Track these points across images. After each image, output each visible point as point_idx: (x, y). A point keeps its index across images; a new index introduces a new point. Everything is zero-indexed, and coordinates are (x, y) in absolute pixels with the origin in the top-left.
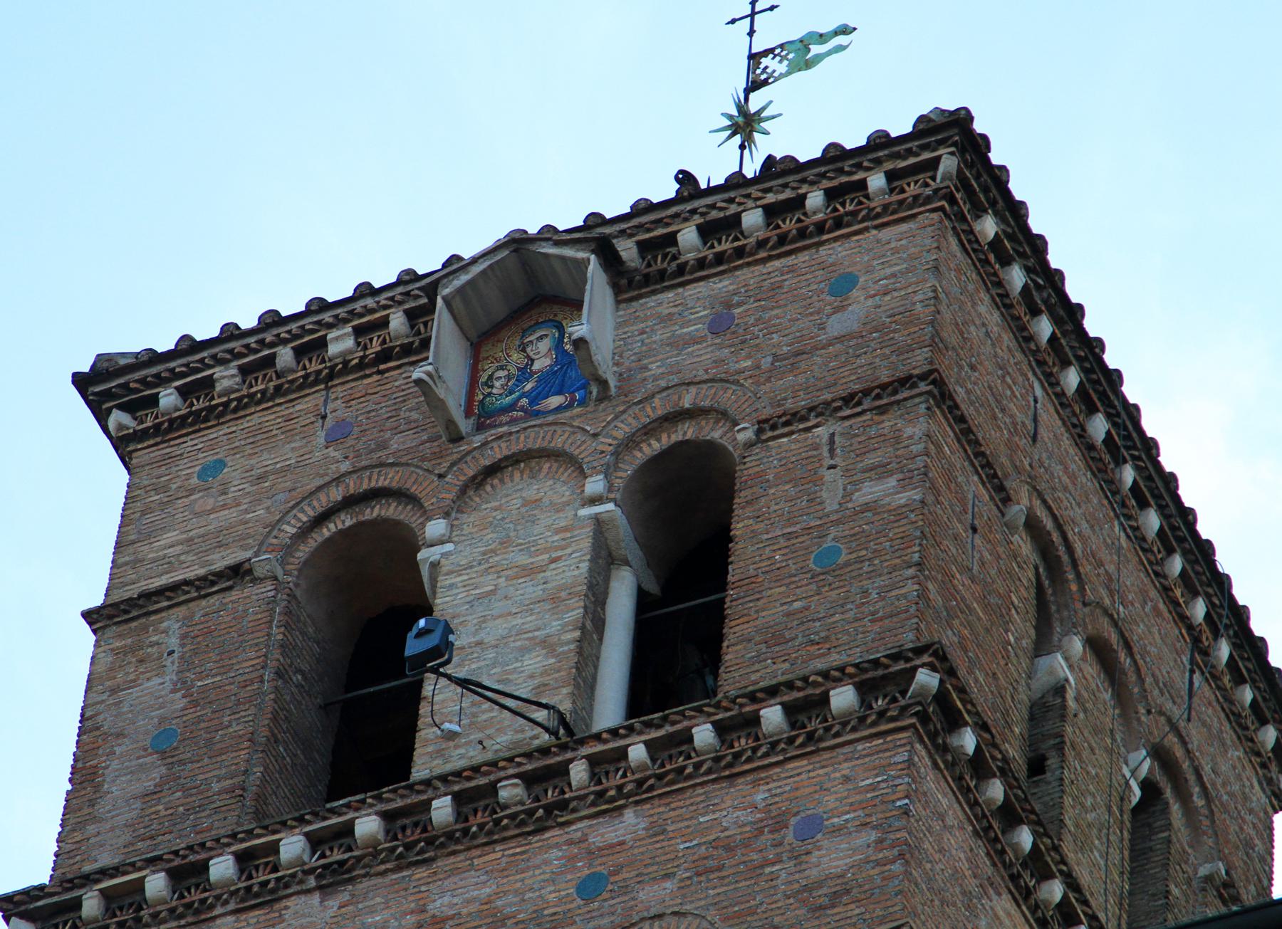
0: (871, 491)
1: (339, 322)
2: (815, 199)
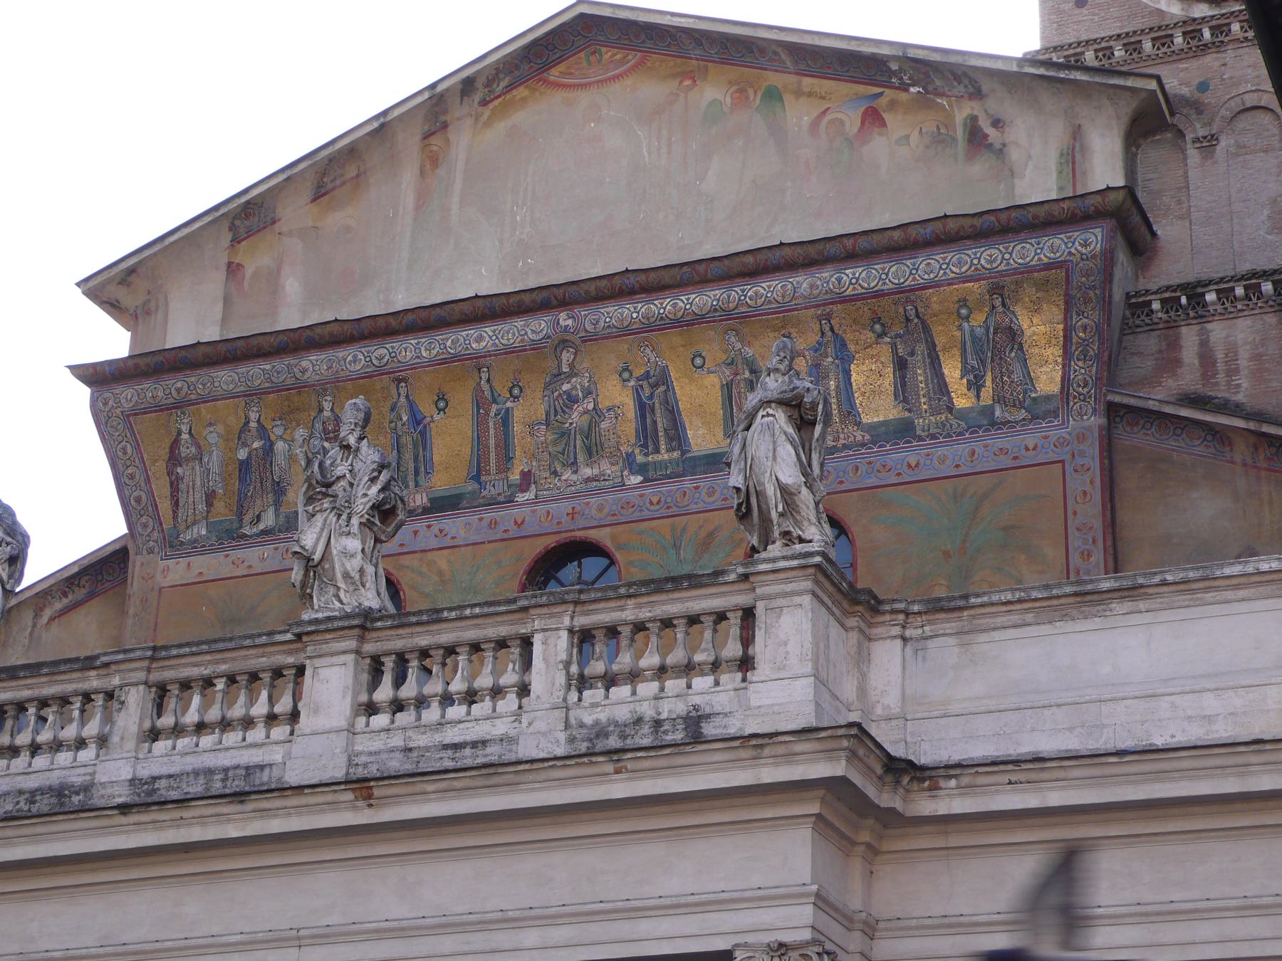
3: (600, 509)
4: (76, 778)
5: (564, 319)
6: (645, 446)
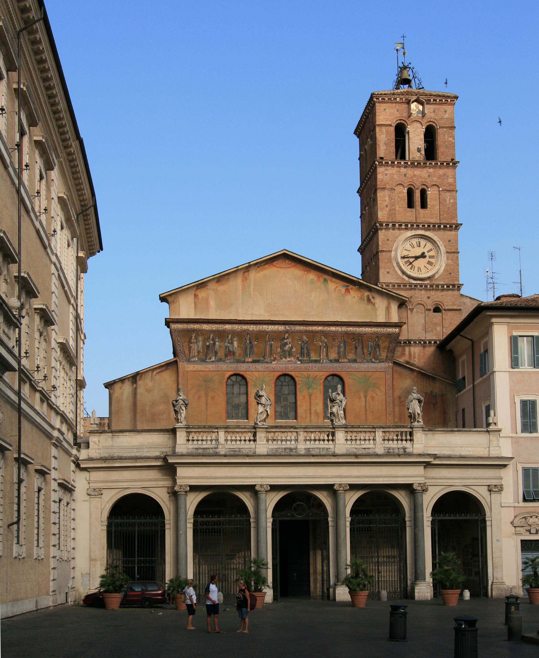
0: (450, 139)
1: (398, 97)
2: (444, 100)
3: (291, 368)
4: (292, 447)
5: (287, 327)
6: (302, 356)
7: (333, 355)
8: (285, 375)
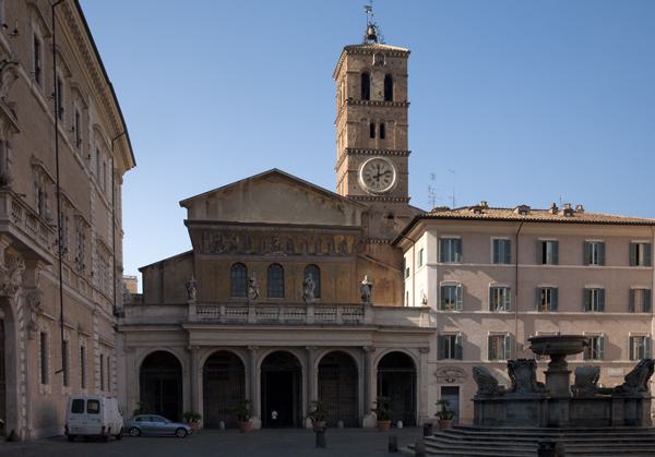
7: (312, 250)
8: (275, 264)
